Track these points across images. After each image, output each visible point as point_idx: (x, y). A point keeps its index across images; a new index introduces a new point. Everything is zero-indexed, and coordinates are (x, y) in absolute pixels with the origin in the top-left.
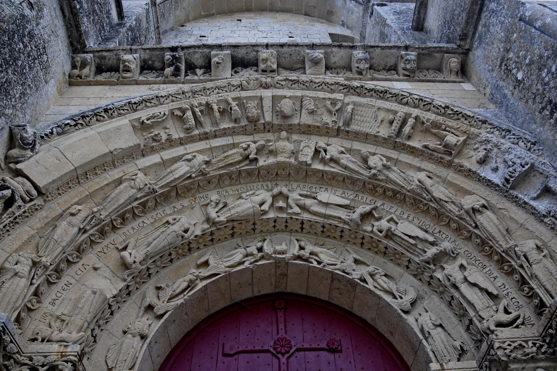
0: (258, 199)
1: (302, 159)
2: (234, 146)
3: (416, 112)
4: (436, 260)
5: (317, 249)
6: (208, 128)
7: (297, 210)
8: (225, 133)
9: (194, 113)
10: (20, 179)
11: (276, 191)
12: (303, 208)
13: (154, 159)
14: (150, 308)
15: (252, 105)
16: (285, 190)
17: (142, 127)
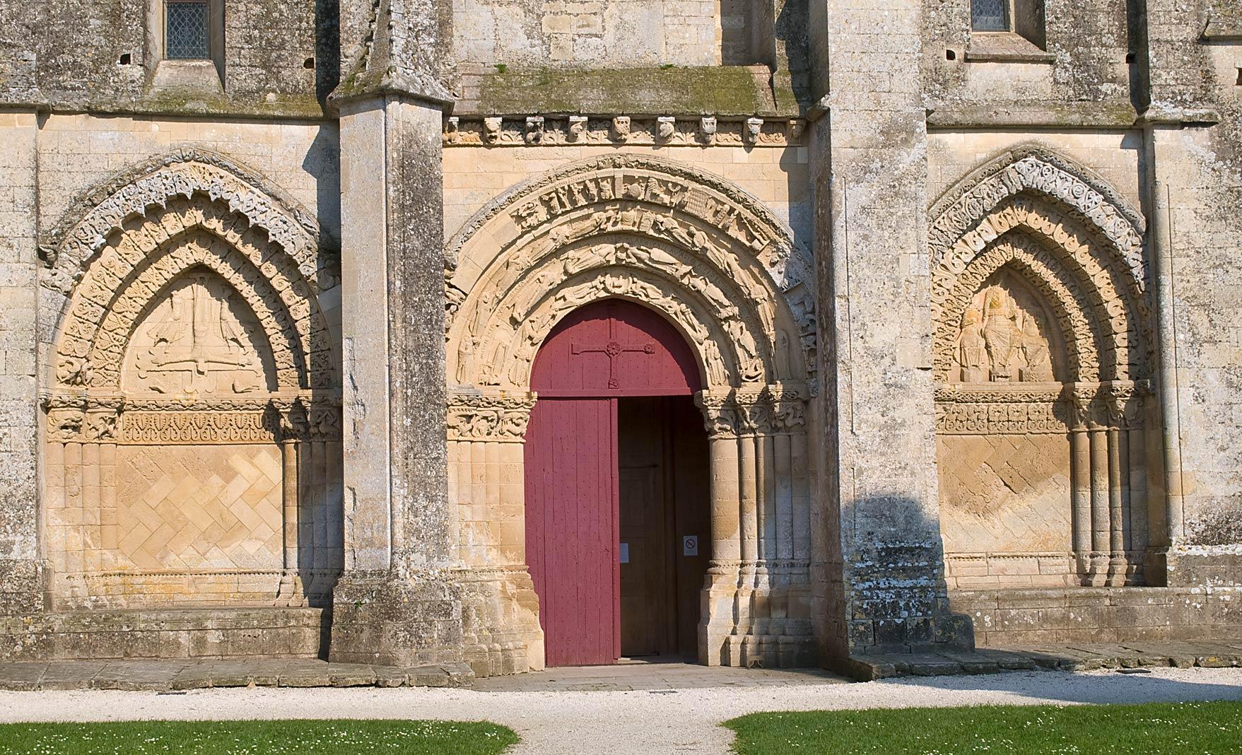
0: (604, 252)
1: (642, 229)
2: (588, 217)
3: (739, 208)
4: (726, 319)
5: (646, 285)
6: (569, 207)
7: (634, 260)
8: (582, 207)
9: (559, 198)
10: (453, 290)
11: (618, 245)
12: (639, 259)
13: (528, 237)
14: (530, 338)
15: (606, 186)
16: (626, 245)
17: (519, 219)
